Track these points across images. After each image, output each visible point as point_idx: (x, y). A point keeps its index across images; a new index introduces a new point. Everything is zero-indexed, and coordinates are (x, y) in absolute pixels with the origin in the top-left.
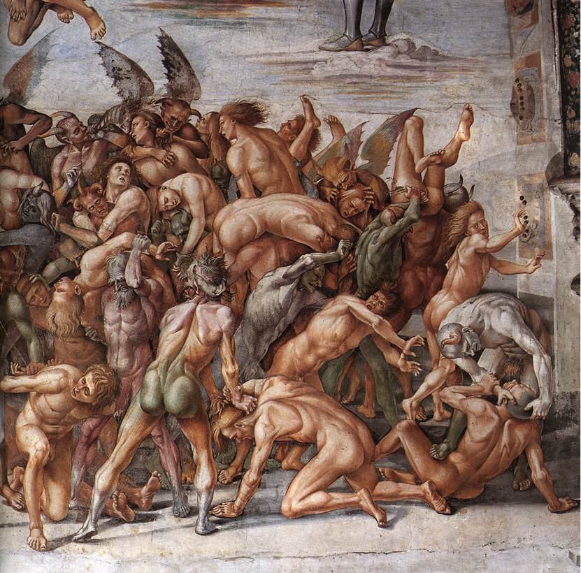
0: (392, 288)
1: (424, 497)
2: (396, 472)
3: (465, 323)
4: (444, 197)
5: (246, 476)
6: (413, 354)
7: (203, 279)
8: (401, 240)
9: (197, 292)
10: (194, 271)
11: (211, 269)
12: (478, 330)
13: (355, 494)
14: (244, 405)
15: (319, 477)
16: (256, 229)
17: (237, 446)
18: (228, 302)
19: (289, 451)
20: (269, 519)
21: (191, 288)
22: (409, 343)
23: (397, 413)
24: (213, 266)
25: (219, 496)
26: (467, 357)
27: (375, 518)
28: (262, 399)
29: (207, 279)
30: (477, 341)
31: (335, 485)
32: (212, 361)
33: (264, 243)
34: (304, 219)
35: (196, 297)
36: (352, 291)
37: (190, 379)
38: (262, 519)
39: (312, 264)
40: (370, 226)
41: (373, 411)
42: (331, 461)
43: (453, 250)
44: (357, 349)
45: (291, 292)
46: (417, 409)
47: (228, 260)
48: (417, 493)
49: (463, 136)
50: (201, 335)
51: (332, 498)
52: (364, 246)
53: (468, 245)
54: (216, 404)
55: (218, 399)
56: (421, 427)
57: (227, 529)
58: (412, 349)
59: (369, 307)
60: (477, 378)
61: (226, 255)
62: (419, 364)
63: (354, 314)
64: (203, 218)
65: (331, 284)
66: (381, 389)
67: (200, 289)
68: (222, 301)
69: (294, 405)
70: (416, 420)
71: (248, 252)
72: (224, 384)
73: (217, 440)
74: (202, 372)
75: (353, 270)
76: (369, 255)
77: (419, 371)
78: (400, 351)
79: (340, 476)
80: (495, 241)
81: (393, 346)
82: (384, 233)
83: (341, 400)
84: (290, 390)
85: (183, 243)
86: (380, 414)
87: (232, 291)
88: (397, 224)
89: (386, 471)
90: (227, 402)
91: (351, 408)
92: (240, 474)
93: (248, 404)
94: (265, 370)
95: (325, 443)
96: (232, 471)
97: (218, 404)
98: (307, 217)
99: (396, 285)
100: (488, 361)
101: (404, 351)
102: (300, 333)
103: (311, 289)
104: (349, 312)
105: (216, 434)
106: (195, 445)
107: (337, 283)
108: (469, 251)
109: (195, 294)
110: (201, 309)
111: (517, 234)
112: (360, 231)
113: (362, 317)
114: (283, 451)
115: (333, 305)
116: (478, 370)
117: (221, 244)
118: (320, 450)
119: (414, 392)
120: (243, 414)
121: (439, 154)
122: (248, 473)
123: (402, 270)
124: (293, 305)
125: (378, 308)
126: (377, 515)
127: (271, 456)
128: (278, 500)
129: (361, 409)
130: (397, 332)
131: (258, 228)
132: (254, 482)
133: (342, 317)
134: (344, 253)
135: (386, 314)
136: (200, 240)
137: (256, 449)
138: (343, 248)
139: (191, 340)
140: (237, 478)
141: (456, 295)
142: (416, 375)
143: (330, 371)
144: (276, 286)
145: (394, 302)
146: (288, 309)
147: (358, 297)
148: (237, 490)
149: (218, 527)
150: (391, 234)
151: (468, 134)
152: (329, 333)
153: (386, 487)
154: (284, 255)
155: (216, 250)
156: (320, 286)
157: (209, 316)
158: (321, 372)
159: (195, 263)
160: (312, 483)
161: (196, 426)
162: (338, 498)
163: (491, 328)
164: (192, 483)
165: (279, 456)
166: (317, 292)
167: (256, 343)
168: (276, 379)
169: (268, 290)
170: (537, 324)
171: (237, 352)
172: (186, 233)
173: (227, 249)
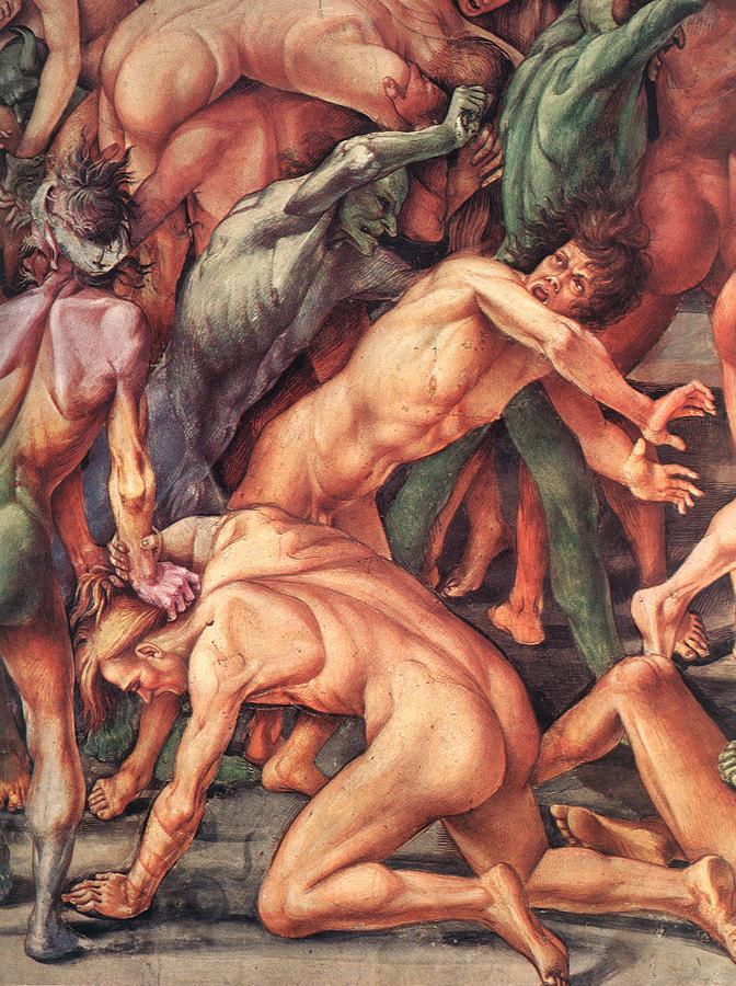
0: (612, 232)
1: (694, 908)
2: (604, 821)
5: (160, 803)
6: (676, 442)
7: (70, 227)
8: (646, 74)
9: (53, 265)
10: (48, 205)
11: (88, 195)
13: (475, 881)
14: (163, 593)
15: (367, 820)
16: (215, 73)
17: (140, 709)
18: (133, 292)
19: (286, 734)
20: (221, 932)
21: (40, 252)
22: (664, 408)
23: (613, 632)
24: (97, 185)
25: (90, 852)
27: (532, 960)
28: (214, 575)
29: (81, 225)
31: (410, 848)
32: (85, 463)
33: (242, 109)
34: (350, 32)
35: (51, 280)
36: (489, 246)
37: (27, 512)
38: (202, 930)
39: (369, 165)
40: (550, 36)
41: (538, 624)
42: (407, 771)
44: (499, 427)
45: (306, 257)
46: (680, 622)
47: (138, 169)
48: (670, 893)
50: (61, 384)
51: (402, 889)
52: (528, 101)
54: (90, 588)
55: (97, 572)
56: (691, 684)
57: (108, 951)
58: (672, 426)
59: (539, 294)
61: (133, 156)
62: (693, 475)
63: (492, 317)
64: (76, 49)
65: (425, 226)
66: (567, 556)
67: (62, 255)
68: (119, 288)
69: (304, 597)
70: (676, 658)
71: (193, 142)
72: (112, 529)
73: (87, 689)
74: (60, 493)
75: (492, 179)
76: (543, 131)
77: (692, 497)
78: (632, 432)
79: (430, 822)
81: (612, 416)
82: (591, 57)
83: (440, 587)
84: (295, 550)
85: (23, 126)
86: (558, 632)
87: (145, 260)
88: (636, 22)
89: (573, 813)
90: (118, 583)
91: (475, 610)
92: (145, 794)
93: (173, 590)
94: (228, 491)
95: (388, 717)
96: (124, 782)
97: (96, 587)
98: (358, 25)
99: (626, 221)
101: (647, 434)
102: (330, 378)
103: (364, 243)
104: (477, 311)
105: (87, 677)
106: (34, 705)
107: (445, 224)
109: (49, 269)
110: (63, 313)
112: (516, 55)
113: (515, 324)
114: (266, 736)
115: (431, 288)
117: (119, 125)
118: (372, 739)
119: (671, 566)
120: (160, 620)
122: (167, 791)
123: (644, 169)
124: (314, 294)
125: (569, 293)
126: (543, 957)
127: (234, 747)
128: (251, 881)
129: (501, 616)
130: (625, 370)
131: (221, 67)
132: (183, 822)
133: (458, 325)
134: (466, 128)
135: (591, 315)
136: (68, 112)
137: (193, 723)
138: (465, 112)
139: (38, 399)
140: (138, 807)
142: (681, 510)
143: (413, 492)
144: (267, 238)
145: (619, 274)
146: (296, 305)
147: (506, 262)
148: (137, 840)
149: (84, 943)
150: (613, 59)
152: (413, 377)
153: (570, 869)
154: (292, 143)
155: (108, 140)
156: (392, 232)
157: (81, 330)
158: (385, 499)
159: (52, 181)
160: (349, 833)
161: (36, 647)
162: (425, 889)
164: (21, 811)
165: (256, 748)
166: (382, 254)
167: (205, 411)
168: (251, 518)
169: (242, 252)
171: (154, 437)
172: (31, 97)
173: (135, 136)
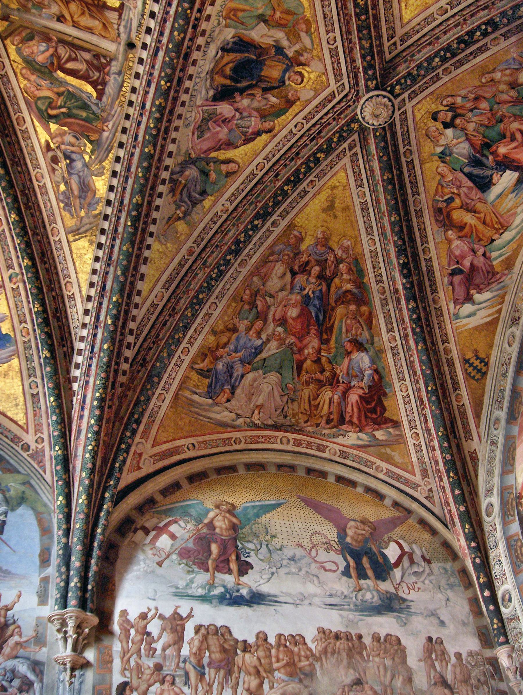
3: (8, 668)
4: (6, 621)
12: (13, 671)
26: (7, 681)
30: (12, 675)
43: (7, 641)
49: (16, 600)
53: (13, 640)
60: (10, 690)
80: (24, 639)
100: (16, 683)
108: (13, 642)
111: (34, 637)
116: (11, 687)
121: (6, 606)
141: (6, 658)
151: (18, 601)
163: (18, 671)
170: (38, 670)
